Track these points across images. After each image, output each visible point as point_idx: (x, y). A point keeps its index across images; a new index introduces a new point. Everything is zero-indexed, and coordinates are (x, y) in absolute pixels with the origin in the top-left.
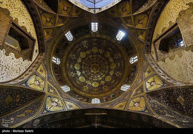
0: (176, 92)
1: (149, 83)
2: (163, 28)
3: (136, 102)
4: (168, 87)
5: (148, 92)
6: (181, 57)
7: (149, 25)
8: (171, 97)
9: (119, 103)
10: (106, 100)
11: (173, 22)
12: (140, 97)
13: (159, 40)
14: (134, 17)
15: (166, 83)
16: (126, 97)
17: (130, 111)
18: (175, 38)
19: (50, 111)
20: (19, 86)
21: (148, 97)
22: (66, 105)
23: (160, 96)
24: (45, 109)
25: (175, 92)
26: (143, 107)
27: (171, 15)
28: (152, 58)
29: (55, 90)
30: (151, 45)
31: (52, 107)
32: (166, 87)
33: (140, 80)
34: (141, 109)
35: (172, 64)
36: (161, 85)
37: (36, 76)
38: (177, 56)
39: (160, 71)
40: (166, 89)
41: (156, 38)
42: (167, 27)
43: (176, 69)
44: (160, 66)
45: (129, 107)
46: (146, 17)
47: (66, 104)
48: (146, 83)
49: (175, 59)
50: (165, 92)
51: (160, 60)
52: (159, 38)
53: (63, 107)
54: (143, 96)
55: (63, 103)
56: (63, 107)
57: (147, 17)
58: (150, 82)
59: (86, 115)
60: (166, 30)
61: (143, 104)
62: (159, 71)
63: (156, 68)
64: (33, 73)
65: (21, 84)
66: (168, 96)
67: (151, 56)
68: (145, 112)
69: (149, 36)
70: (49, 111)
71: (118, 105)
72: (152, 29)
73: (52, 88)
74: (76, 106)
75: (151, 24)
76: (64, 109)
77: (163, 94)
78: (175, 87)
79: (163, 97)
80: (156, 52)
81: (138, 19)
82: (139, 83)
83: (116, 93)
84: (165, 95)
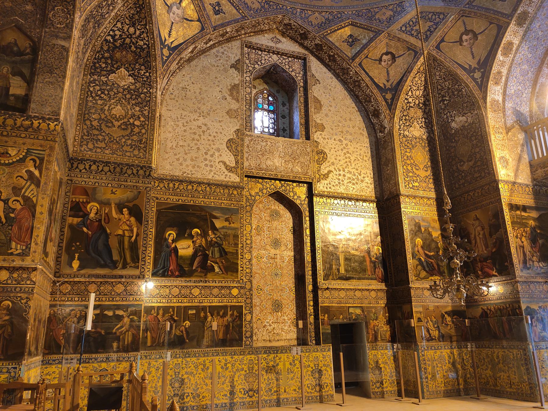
0: (143, 75)
2: (321, 106)
4: (159, 59)
6: (228, 113)
7: (357, 78)
8: (130, 57)
11: (319, 133)
13: (299, 78)
14: (416, 53)
15: (170, 54)
18: (283, 111)
25: (144, 73)
27: (335, 137)
30: (302, 45)
32: (158, 52)
35: (218, 86)
36: (167, 38)
38: (234, 105)
40: (155, 51)
41: (310, 71)
42: (318, 115)
43: (204, 88)
46: (386, 83)
49: (228, 97)
50: (145, 44)
51: (242, 54)
52: (306, 82)
57: (382, 85)
60: (312, 110)
63: (222, 35)
66: (133, 48)
69: (329, 56)
72: (344, 74)
75: (357, 81)
77: (139, 36)
78: (156, 78)
79: (131, 35)
80: (273, 53)
81: (401, 58)
84: (137, 42)
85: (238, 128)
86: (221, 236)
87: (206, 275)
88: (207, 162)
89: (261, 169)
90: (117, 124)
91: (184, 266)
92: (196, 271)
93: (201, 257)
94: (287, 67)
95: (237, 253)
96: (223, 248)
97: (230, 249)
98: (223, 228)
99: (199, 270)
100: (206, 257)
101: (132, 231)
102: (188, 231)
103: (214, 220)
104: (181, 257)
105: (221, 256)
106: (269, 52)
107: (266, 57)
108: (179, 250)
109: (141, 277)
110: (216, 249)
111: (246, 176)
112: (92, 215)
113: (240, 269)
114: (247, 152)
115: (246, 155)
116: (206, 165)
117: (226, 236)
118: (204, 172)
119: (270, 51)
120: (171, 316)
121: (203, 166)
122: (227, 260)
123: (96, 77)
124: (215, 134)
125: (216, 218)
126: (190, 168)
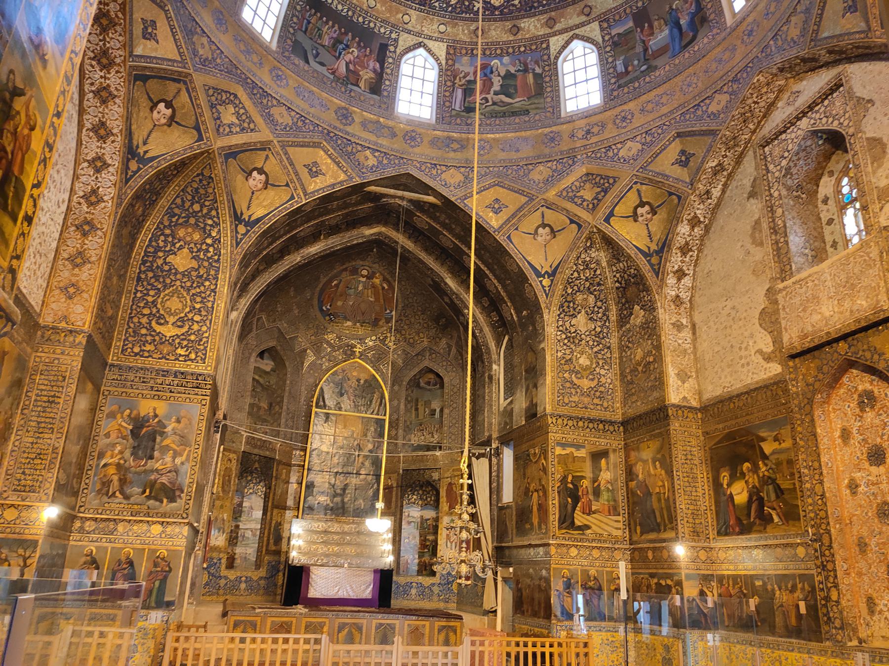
1: (641, 198)
3: (549, 226)
5: (604, 227)
9: (497, 185)
10: (468, 91)
12: (572, 222)
15: (661, 257)
16: (540, 173)
17: (510, 248)
19: (252, 219)
20: (130, 193)
21: (589, 238)
22: (294, 168)
23: (619, 261)
24: (237, 218)
26: (550, 260)
28: (771, 106)
29: (236, 96)
31: (254, 197)
33: (638, 138)
34: (543, 263)
37: (144, 79)
39: (716, 192)
44: (738, 177)
45: (517, 229)
47: (298, 167)
48: (631, 187)
53: (287, 185)
54: (580, 226)
55: (285, 168)
56: (287, 185)
58: (644, 200)
59: (370, 193)
61: (558, 249)
62: (708, 192)
64: (130, 82)
65: (127, 174)
67: (780, 91)
68: (541, 282)
70: (250, 224)
71: (490, 195)
73: (224, 98)
74: (336, 168)
76: (292, 198)
80: (798, 119)
82: (621, 154)
83: (526, 70)
85: (767, 287)
86: (774, 466)
87: (765, 529)
88: (743, 361)
89: (806, 336)
90: (640, 369)
91: (742, 518)
92: (754, 523)
93: (756, 502)
94: (825, 120)
95: (795, 488)
96: (778, 485)
97: (785, 485)
98: (774, 453)
99: (758, 521)
100: (761, 501)
101: (664, 486)
102: (739, 468)
103: (762, 444)
104: (738, 505)
105: (777, 497)
106: (793, 124)
107: (793, 135)
108: (735, 497)
109: (676, 539)
110: (771, 487)
111: (793, 357)
112: (640, 476)
113: (802, 514)
114: (784, 318)
115: (783, 323)
116: (743, 366)
117: (778, 464)
118: (743, 377)
119: (792, 123)
120: (741, 588)
121: (740, 369)
122: (786, 503)
123: (624, 329)
124: (745, 314)
125: (763, 440)
126: (729, 379)
